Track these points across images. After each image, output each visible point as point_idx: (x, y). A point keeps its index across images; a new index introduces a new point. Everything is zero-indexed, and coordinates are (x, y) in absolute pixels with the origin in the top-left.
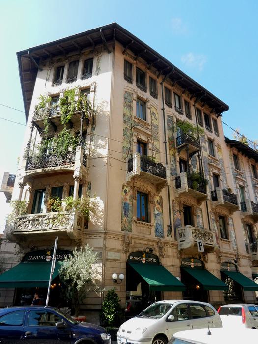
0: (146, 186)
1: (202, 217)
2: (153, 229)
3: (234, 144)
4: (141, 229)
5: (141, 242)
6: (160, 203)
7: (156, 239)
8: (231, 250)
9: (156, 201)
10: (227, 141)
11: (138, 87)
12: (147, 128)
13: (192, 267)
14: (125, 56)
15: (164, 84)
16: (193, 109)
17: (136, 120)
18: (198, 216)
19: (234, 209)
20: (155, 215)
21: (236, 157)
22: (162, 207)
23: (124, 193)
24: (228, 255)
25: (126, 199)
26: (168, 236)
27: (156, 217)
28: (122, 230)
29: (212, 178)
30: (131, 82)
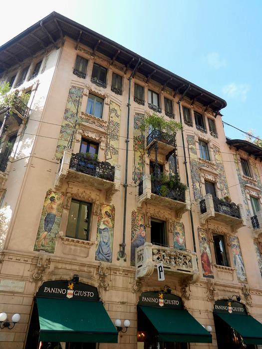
0: (88, 192)
1: (184, 235)
2: (93, 250)
3: (238, 144)
4: (71, 249)
5: (64, 266)
6: (111, 215)
7: (96, 263)
8: (234, 282)
9: (103, 212)
10: (231, 143)
11: (93, 82)
12: (101, 126)
13: (230, 312)
14: (78, 51)
15: (133, 81)
16: (176, 107)
17: (83, 116)
18: (177, 233)
19: (237, 224)
20: (99, 231)
21: (245, 163)
22: (113, 219)
23: (49, 201)
24: (228, 289)
25: (52, 208)
26: (118, 259)
27: (100, 233)
28: (36, 250)
29: (203, 186)
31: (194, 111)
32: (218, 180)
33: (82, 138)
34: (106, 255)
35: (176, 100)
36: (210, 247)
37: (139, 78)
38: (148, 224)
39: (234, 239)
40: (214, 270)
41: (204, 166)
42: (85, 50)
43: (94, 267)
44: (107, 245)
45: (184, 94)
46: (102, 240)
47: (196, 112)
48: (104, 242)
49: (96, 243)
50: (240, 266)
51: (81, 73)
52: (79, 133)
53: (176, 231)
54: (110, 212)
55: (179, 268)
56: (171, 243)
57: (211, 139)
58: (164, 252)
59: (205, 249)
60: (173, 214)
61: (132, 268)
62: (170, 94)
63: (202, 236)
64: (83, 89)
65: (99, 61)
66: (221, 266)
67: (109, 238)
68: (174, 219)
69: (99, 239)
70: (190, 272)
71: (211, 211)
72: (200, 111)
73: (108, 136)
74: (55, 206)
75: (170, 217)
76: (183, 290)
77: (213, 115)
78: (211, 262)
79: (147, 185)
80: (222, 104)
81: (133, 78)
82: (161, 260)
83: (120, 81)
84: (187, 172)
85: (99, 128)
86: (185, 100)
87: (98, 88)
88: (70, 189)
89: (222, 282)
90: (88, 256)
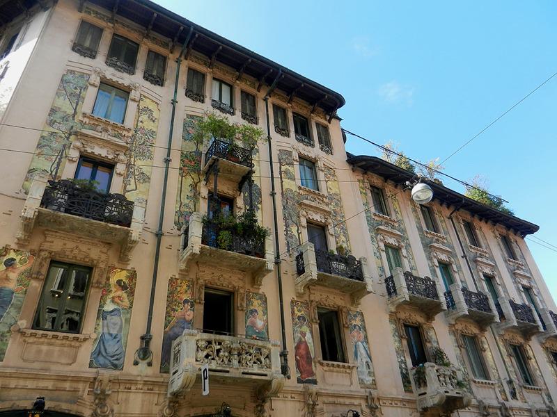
0: (84, 248)
1: (265, 313)
2: (86, 351)
3: (364, 163)
4: (39, 352)
5: (22, 383)
6: (128, 287)
7: (91, 373)
8: (353, 388)
9: (113, 280)
10: (355, 162)
11: (109, 63)
12: (119, 136)
14: (83, 15)
16: (261, 105)
17: (86, 120)
18: (254, 312)
19: (358, 291)
20: (102, 315)
22: (131, 294)
24: (341, 400)
25: (7, 279)
27: (104, 318)
29: (305, 232)
30: (288, 135)
31: (293, 113)
32: (330, 221)
33: (81, 157)
34: (112, 357)
35: (261, 95)
36: (311, 332)
37: (198, 60)
38: (199, 298)
39: (355, 316)
40: (318, 370)
41: (307, 199)
42: (97, 13)
43: (85, 380)
44: (117, 339)
45: (274, 84)
46: (106, 330)
47: (295, 115)
48: (111, 335)
49: (94, 336)
50: (364, 360)
51: (88, 49)
52: (76, 148)
53: (252, 308)
54: (127, 281)
55: (246, 371)
56: (241, 329)
57: (320, 156)
58: (220, 344)
59: (304, 335)
60: (248, 279)
61: (162, 377)
62: (253, 85)
63: (299, 314)
64: (89, 75)
65: (123, 31)
66: (335, 363)
67: (121, 328)
68: (248, 287)
69: (100, 330)
70: (266, 375)
71: (312, 271)
72: (303, 112)
73: (133, 153)
74: (13, 276)
75: (241, 284)
76: (259, 408)
77: (326, 119)
78: (312, 356)
79: (196, 231)
80: (338, 101)
81: (186, 59)
82: (213, 359)
83: (162, 64)
84: (275, 213)
85: (114, 138)
86: (279, 95)
87: (119, 74)
88: (49, 244)
89: (331, 390)
90: (74, 361)
